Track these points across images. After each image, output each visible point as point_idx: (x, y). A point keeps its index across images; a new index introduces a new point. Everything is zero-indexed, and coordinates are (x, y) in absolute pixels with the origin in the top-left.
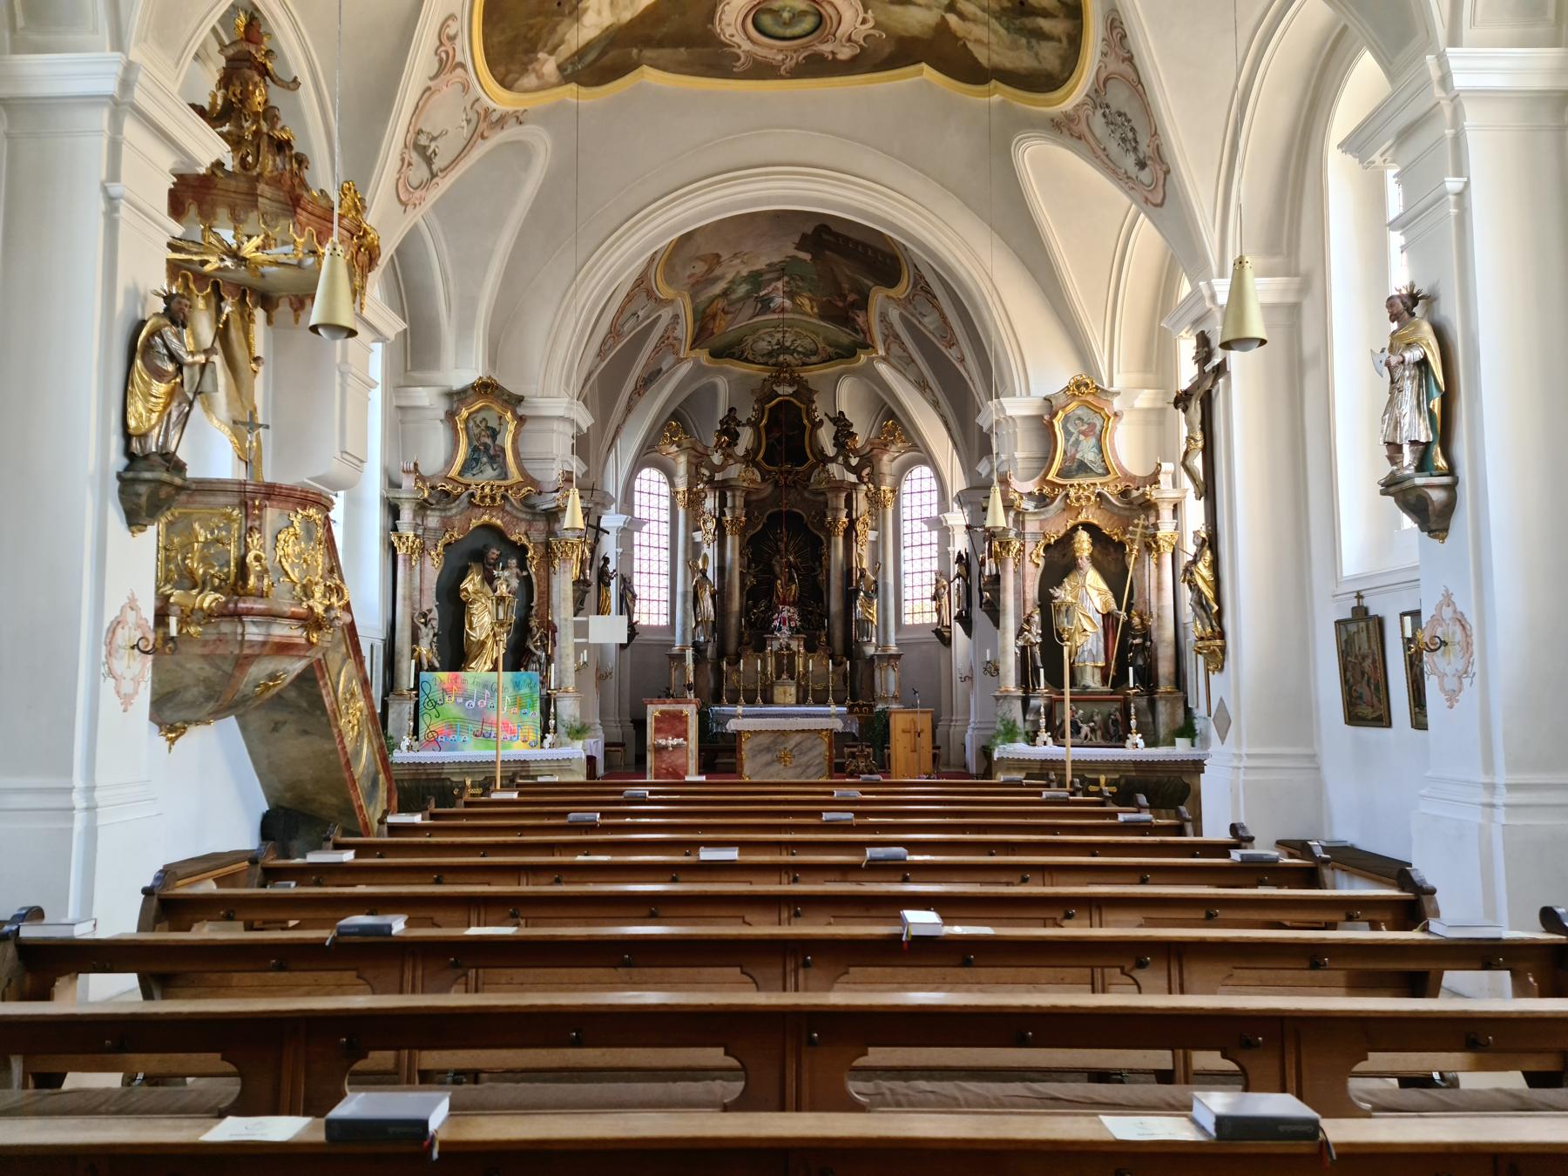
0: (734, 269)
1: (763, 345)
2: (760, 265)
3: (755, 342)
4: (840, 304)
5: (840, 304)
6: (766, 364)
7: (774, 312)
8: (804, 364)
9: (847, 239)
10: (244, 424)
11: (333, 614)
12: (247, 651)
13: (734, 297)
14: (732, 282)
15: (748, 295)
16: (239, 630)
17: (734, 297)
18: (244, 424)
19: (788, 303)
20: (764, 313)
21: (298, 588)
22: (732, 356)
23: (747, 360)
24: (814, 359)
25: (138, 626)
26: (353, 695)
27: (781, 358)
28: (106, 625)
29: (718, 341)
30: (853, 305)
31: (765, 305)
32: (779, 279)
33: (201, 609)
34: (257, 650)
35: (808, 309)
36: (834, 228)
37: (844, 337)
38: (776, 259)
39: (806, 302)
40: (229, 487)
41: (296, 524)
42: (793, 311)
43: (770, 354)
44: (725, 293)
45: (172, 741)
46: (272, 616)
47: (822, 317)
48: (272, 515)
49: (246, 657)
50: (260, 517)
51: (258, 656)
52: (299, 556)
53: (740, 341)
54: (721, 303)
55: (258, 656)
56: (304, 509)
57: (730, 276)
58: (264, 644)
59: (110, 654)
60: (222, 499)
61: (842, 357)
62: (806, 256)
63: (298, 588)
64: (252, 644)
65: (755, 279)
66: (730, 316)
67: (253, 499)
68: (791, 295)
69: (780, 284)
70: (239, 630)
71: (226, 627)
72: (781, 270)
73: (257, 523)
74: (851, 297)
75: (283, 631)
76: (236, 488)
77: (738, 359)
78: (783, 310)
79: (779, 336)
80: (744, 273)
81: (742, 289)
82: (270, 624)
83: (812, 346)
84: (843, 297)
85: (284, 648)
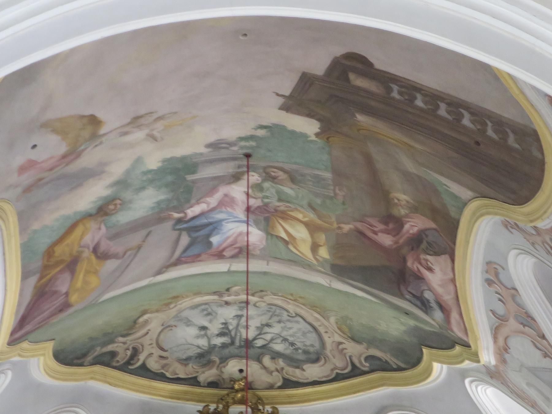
0: (129, 155)
1: (187, 337)
2: (192, 143)
3: (166, 327)
4: (386, 240)
5: (386, 240)
6: (193, 381)
7: (220, 255)
8: (288, 384)
9: (411, 89)
13: (123, 218)
14: (122, 183)
15: (158, 217)
17: (123, 218)
19: (256, 236)
20: (195, 259)
22: (107, 360)
23: (144, 371)
24: (313, 371)
27: (233, 367)
29: (76, 327)
30: (417, 241)
31: (198, 238)
32: (236, 178)
35: (305, 249)
36: (380, 61)
37: (391, 319)
38: (231, 132)
39: (301, 233)
42: (268, 255)
43: (204, 358)
44: (103, 210)
47: (340, 270)
53: (132, 326)
54: (92, 234)
57: (117, 170)
61: (379, 366)
62: (308, 127)
65: (180, 177)
66: (111, 265)
68: (264, 215)
69: (238, 191)
72: (246, 158)
74: (414, 225)
77: (124, 368)
78: (245, 252)
79: (228, 314)
80: (153, 162)
81: (145, 202)
83: (311, 340)
84: (394, 223)
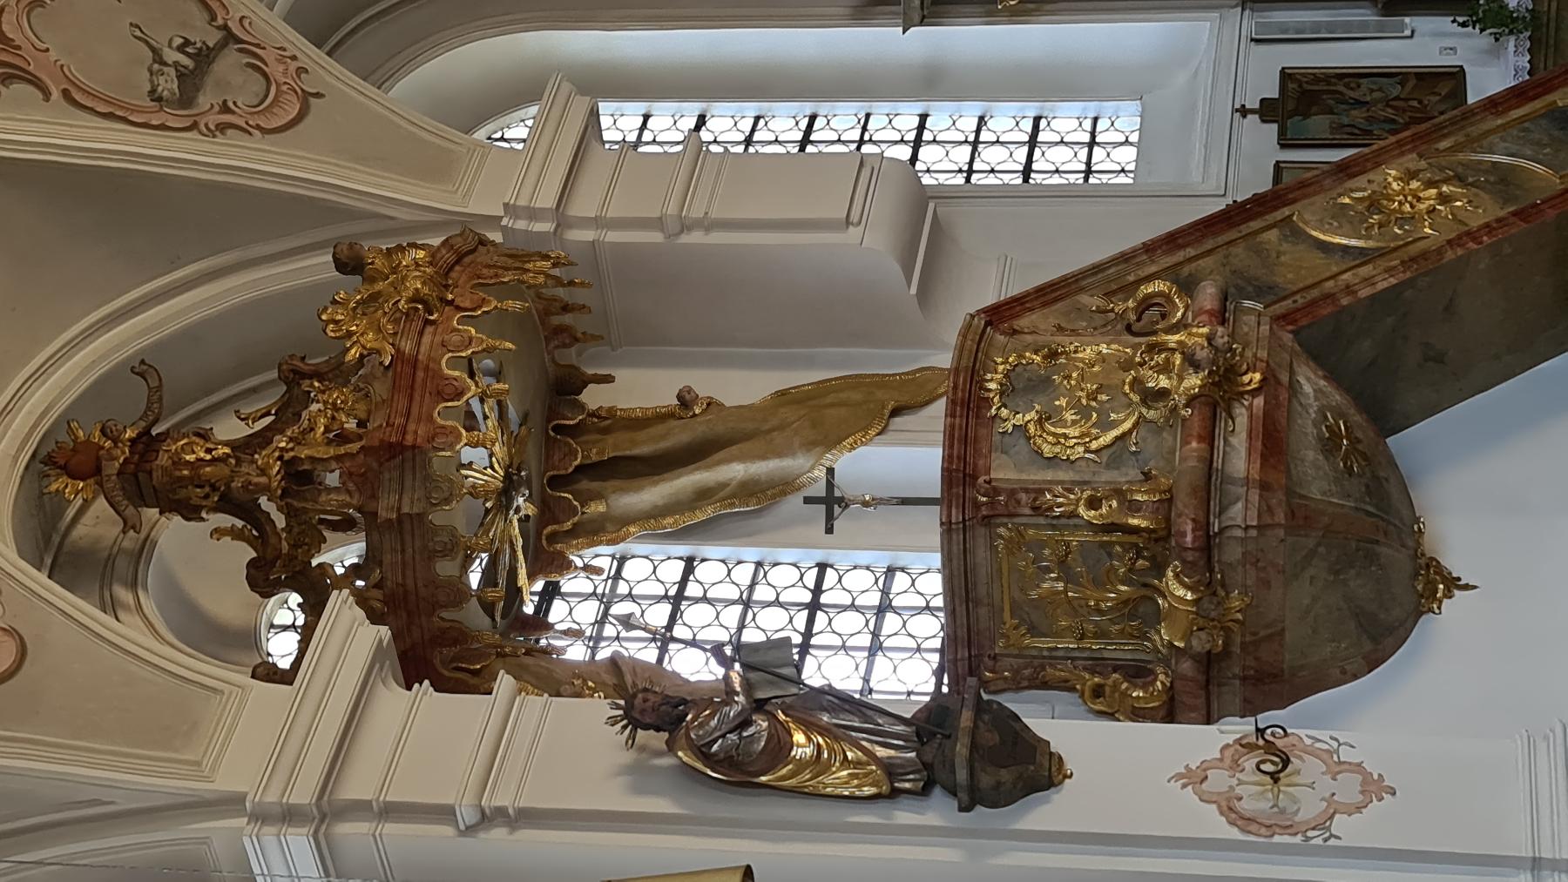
10: (830, 518)
11: (1202, 354)
12: (1280, 517)
16: (1239, 533)
18: (830, 518)
21: (1151, 415)
25: (1235, 766)
26: (1373, 204)
28: (1234, 834)
33: (1196, 602)
34: (1277, 498)
40: (957, 548)
41: (1019, 419)
45: (1453, 584)
46: (1210, 483)
48: (1004, 471)
49: (1292, 514)
50: (1012, 493)
51: (1290, 492)
52: (1084, 412)
55: (1290, 492)
56: (988, 402)
58: (1264, 487)
59: (1288, 829)
60: (981, 555)
63: (1151, 415)
64: (1266, 509)
67: (977, 506)
70: (1239, 533)
71: (1233, 553)
73: (1023, 497)
75: (1238, 456)
76: (958, 537)
82: (1226, 479)
85: (1272, 442)
